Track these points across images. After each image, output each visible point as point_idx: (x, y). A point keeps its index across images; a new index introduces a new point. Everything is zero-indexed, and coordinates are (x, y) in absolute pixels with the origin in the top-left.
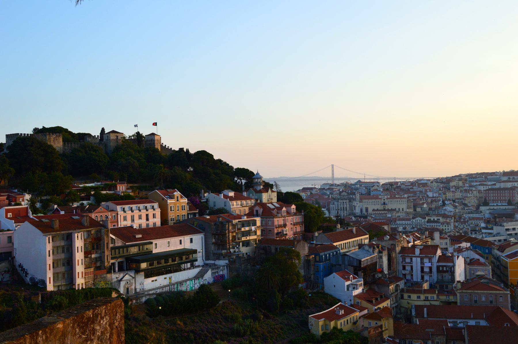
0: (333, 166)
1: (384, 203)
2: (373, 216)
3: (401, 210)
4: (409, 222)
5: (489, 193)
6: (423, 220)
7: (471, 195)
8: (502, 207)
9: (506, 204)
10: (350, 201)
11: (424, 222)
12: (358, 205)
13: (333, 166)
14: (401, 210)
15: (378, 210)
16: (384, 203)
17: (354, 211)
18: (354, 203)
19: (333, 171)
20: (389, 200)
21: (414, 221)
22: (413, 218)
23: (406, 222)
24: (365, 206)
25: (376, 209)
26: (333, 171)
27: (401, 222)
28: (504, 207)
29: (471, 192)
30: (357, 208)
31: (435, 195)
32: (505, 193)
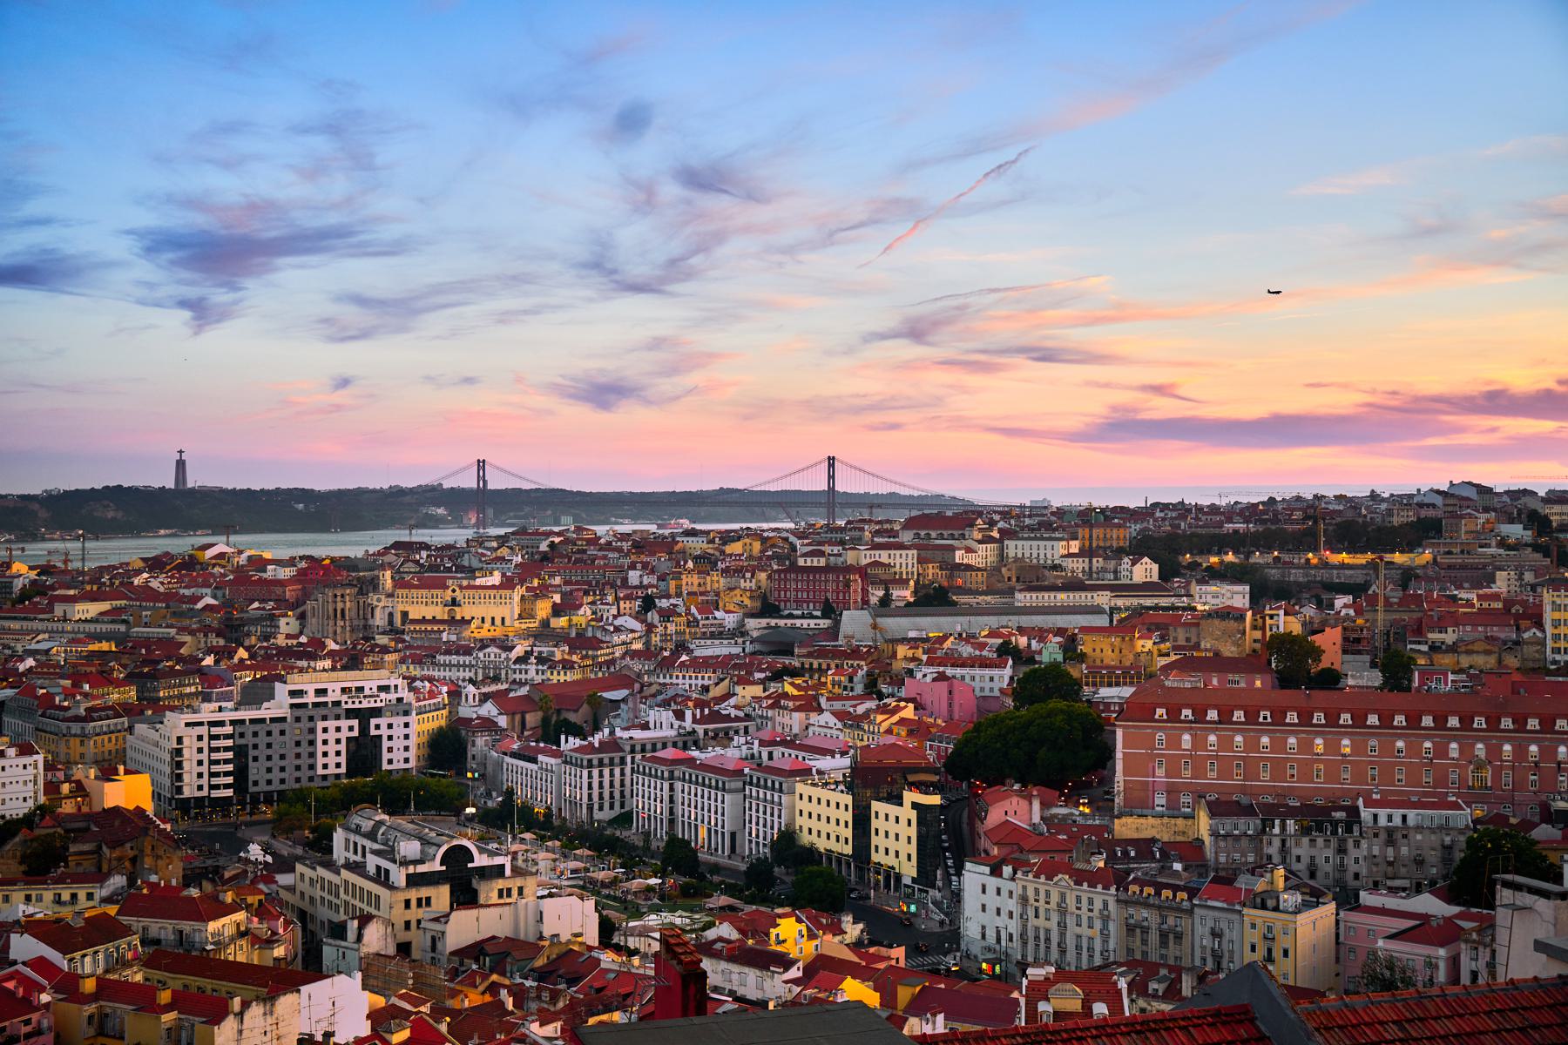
0: (831, 461)
1: (454, 602)
2: (407, 638)
3: (498, 622)
4: (467, 659)
5: (786, 580)
6: (504, 656)
7: (748, 585)
8: (805, 623)
9: (818, 613)
10: (361, 592)
11: (508, 659)
12: (381, 604)
13: (831, 461)
14: (498, 622)
15: (434, 621)
16: (454, 600)
17: (371, 622)
18: (373, 599)
19: (831, 477)
20: (466, 592)
21: (481, 655)
22: (480, 649)
23: (461, 659)
24: (401, 607)
25: (429, 617)
26: (831, 477)
27: (447, 658)
28: (812, 622)
29: (748, 575)
30: (378, 612)
31: (646, 581)
32: (826, 581)
